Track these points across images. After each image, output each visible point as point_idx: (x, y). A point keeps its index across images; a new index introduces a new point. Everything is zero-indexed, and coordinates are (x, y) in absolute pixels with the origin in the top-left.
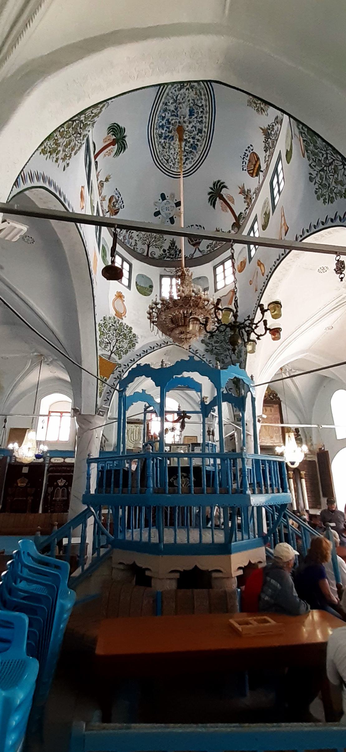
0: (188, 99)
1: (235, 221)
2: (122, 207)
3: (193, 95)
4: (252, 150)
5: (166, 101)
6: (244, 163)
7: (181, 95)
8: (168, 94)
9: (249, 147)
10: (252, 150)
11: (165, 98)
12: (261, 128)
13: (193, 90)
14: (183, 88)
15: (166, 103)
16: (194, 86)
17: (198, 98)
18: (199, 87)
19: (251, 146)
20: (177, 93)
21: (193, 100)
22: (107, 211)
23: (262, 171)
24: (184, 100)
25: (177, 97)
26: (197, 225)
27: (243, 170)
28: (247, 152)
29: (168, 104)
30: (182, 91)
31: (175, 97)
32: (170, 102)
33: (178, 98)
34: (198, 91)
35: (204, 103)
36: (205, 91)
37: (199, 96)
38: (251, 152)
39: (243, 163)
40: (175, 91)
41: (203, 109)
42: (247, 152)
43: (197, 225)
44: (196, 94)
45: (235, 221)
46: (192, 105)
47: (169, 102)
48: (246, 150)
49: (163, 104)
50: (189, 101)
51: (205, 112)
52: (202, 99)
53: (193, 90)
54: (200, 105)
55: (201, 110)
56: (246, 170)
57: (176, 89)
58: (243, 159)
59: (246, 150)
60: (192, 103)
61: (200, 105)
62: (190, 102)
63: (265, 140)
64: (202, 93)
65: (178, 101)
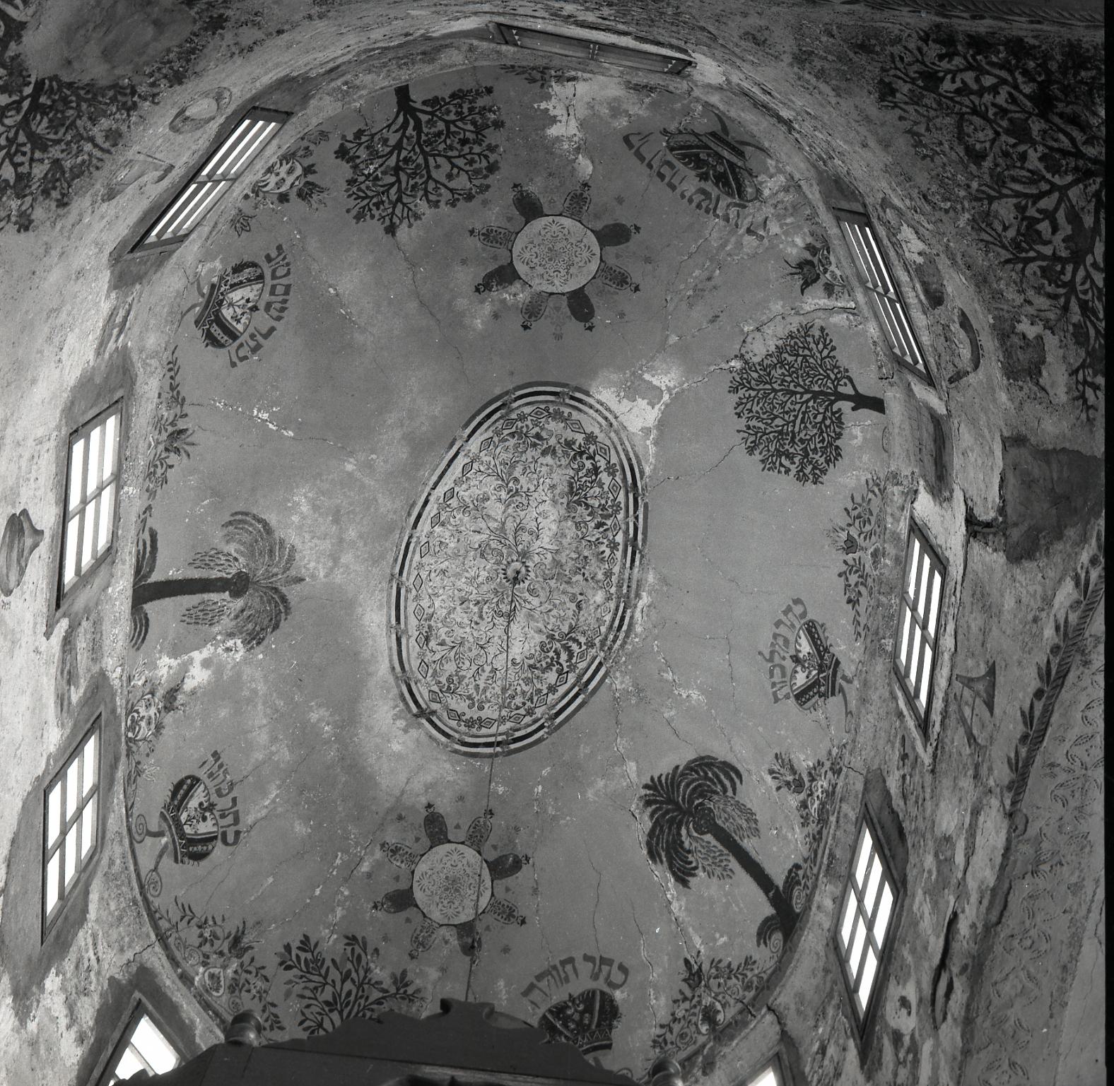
1: (769, 910)
2: (230, 838)
4: (804, 614)
6: (777, 671)
9: (788, 610)
10: (804, 614)
19: (797, 601)
22: (154, 827)
26: (587, 958)
27: (777, 700)
28: (782, 630)
39: (772, 676)
42: (782, 630)
43: (587, 958)
45: (769, 910)
48: (778, 624)
56: (787, 696)
58: (771, 660)
59: (778, 624)
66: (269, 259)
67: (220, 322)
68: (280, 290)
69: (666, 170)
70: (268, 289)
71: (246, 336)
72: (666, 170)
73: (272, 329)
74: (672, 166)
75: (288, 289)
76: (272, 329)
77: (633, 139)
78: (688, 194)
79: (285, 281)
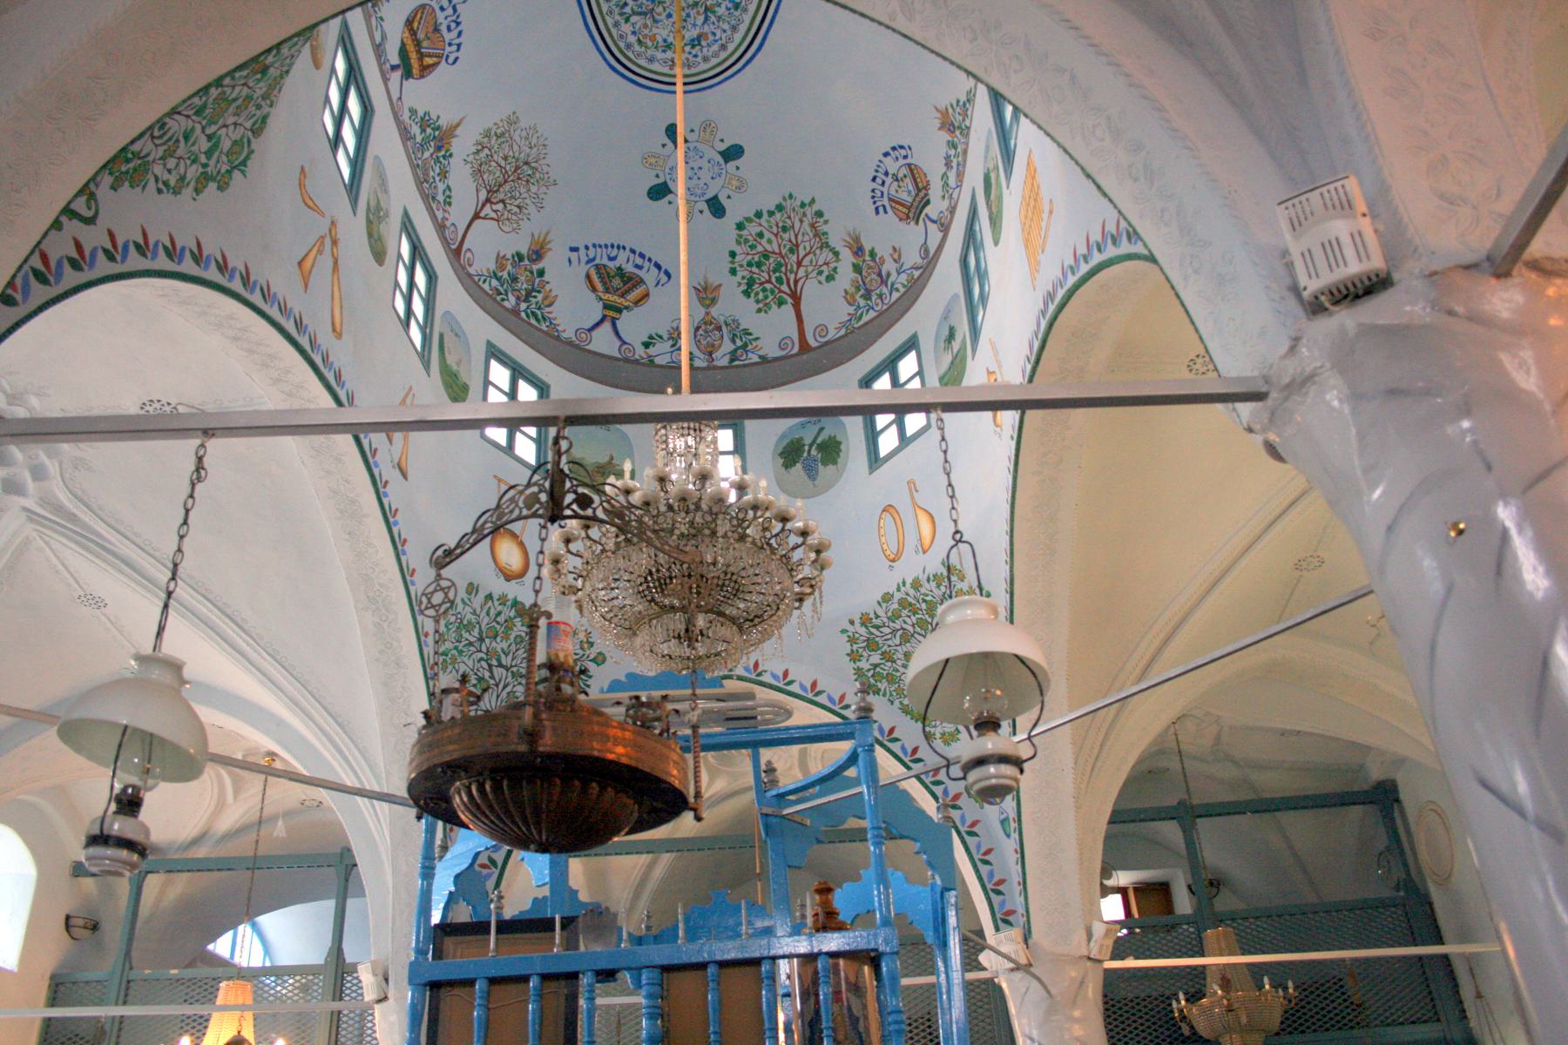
0: (671, 20)
3: (661, 31)
5: (737, 13)
7: (694, 25)
8: (734, 29)
11: (740, 21)
12: (458, 125)
13: (665, 41)
14: (693, 40)
15: (736, 9)
16: (664, 51)
17: (646, 31)
18: (650, 53)
20: (706, 29)
21: (656, 21)
23: (394, 68)
24: (684, 14)
25: (706, 19)
29: (730, 5)
30: (694, 33)
31: (713, 19)
32: (723, 6)
33: (702, 18)
34: (650, 44)
35: (626, 28)
36: (630, 54)
37: (645, 36)
38: (448, 49)
40: (714, 34)
41: (621, 14)
44: (653, 38)
46: (660, 9)
47: (728, 9)
48: (460, 34)
49: (745, 10)
50: (669, 16)
51: (617, 11)
52: (634, 33)
53: (665, 41)
54: (634, 19)
55: (628, 10)
57: (711, 38)
59: (460, 34)
60: (659, 14)
61: (634, 19)
62: (664, 15)
63: (438, 128)
64: (637, 48)
65: (702, 10)
66: (886, 212)
67: (919, 190)
68: (879, 181)
69: (639, 261)
70: (887, 184)
71: (901, 161)
72: (639, 261)
73: (886, 154)
74: (637, 266)
75: (874, 179)
76: (886, 154)
77: (664, 278)
78: (622, 250)
79: (874, 185)
